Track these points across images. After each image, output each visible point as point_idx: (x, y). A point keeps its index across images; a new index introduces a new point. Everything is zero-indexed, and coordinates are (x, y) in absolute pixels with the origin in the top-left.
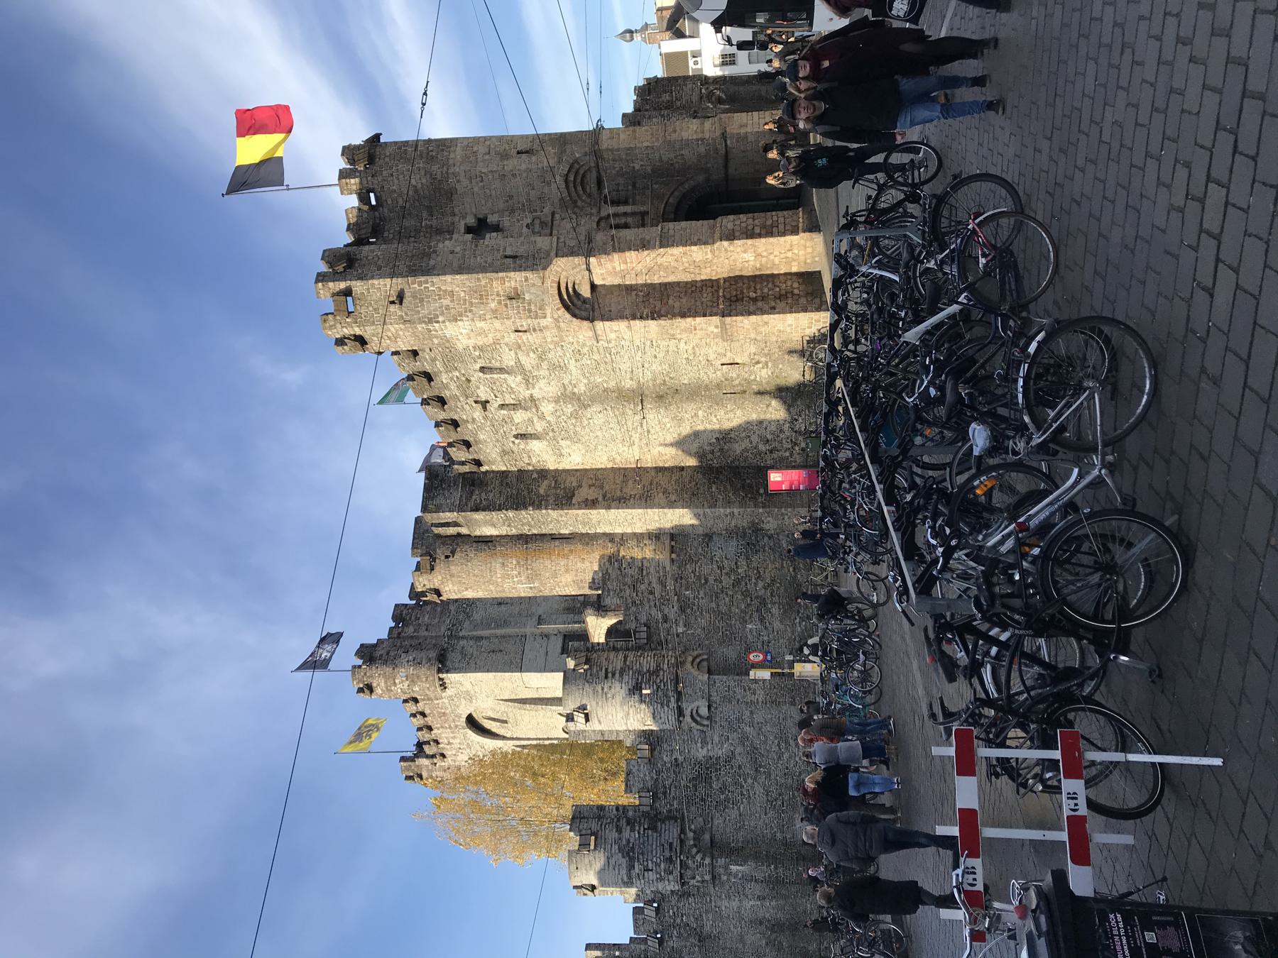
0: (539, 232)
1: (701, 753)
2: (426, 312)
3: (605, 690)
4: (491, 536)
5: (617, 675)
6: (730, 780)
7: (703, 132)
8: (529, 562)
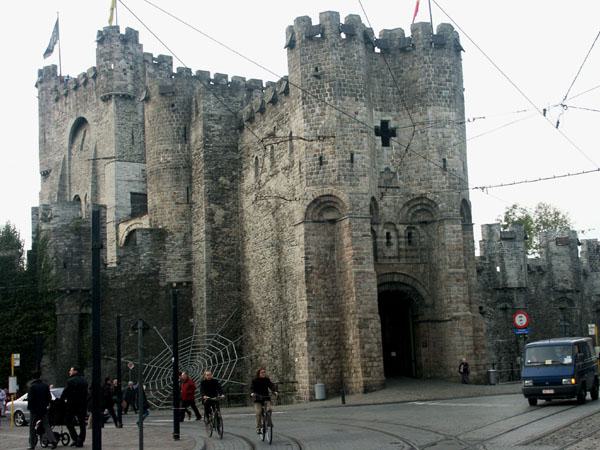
4: (189, 140)
7: (457, 302)
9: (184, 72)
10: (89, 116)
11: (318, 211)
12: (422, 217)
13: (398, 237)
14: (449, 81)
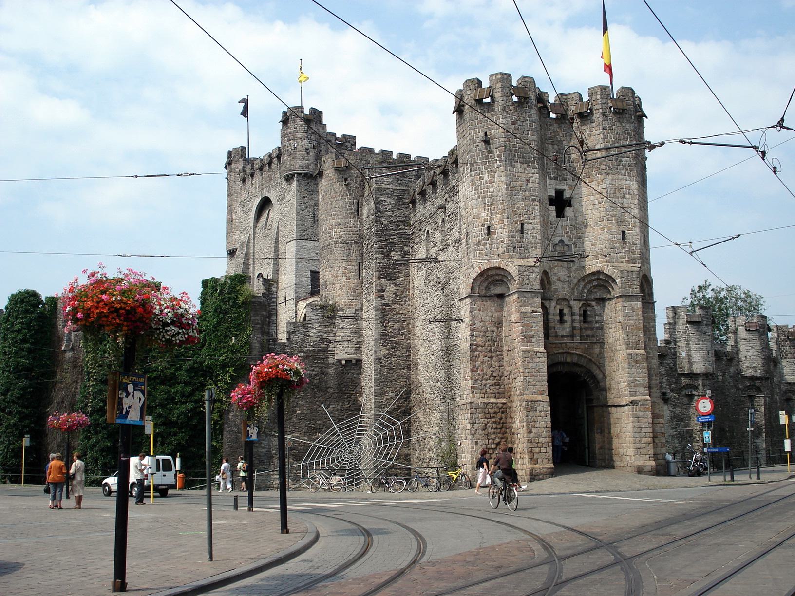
0: (555, 250)
10: (272, 195)
11: (485, 284)
13: (573, 314)
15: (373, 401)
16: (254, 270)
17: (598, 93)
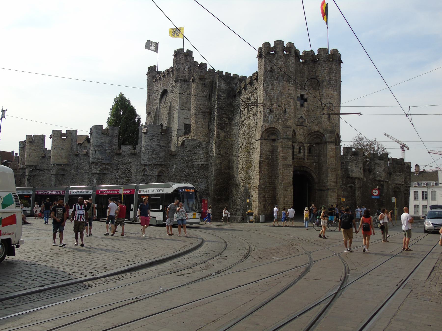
1: (133, 171)
2: (267, 80)
3: (153, 139)
5: (158, 144)
6: (124, 181)
7: (330, 182)
8: (201, 113)
9: (212, 71)
11: (268, 134)
12: (316, 141)
14: (335, 77)
15: (213, 183)
16: (159, 122)
17: (322, 51)
